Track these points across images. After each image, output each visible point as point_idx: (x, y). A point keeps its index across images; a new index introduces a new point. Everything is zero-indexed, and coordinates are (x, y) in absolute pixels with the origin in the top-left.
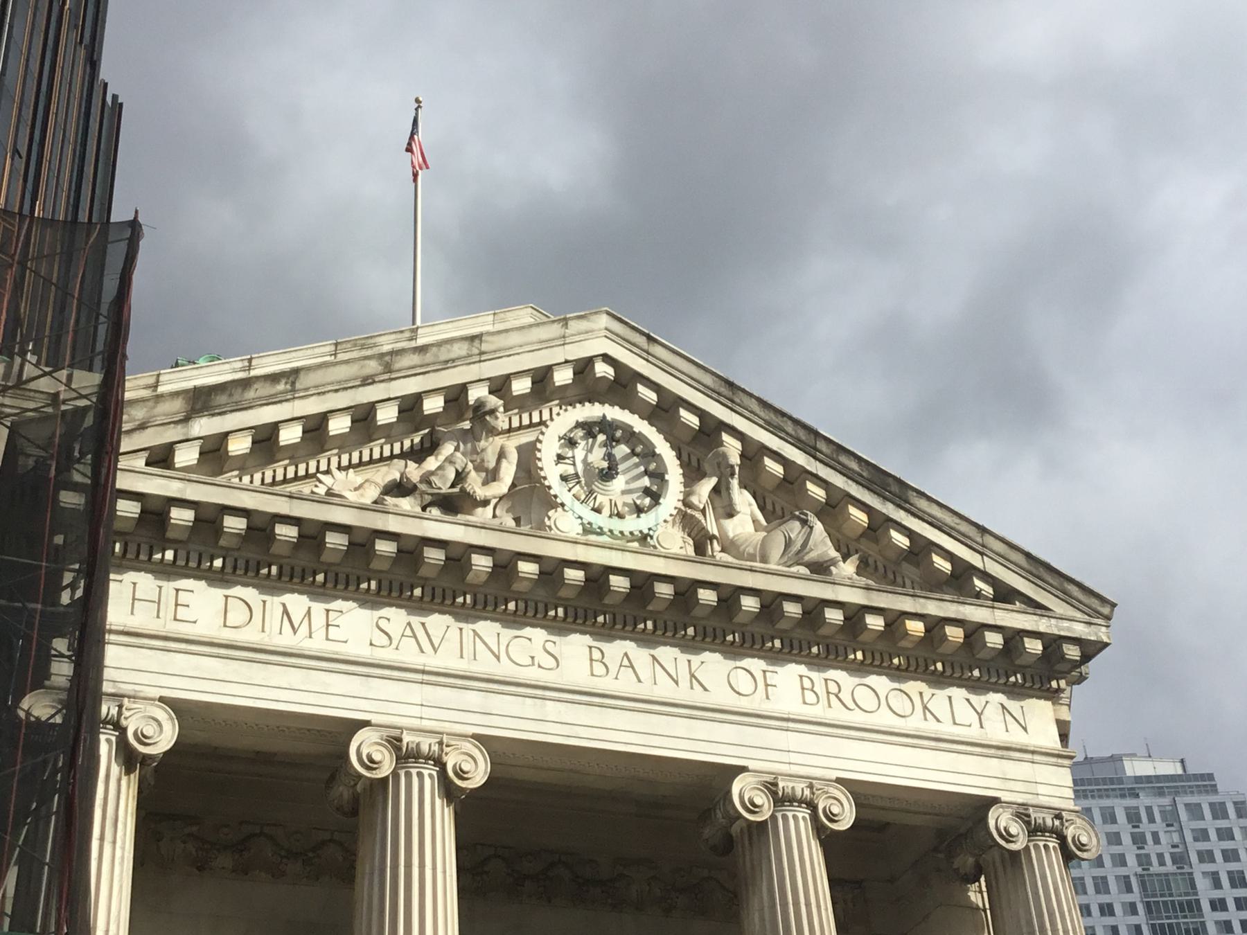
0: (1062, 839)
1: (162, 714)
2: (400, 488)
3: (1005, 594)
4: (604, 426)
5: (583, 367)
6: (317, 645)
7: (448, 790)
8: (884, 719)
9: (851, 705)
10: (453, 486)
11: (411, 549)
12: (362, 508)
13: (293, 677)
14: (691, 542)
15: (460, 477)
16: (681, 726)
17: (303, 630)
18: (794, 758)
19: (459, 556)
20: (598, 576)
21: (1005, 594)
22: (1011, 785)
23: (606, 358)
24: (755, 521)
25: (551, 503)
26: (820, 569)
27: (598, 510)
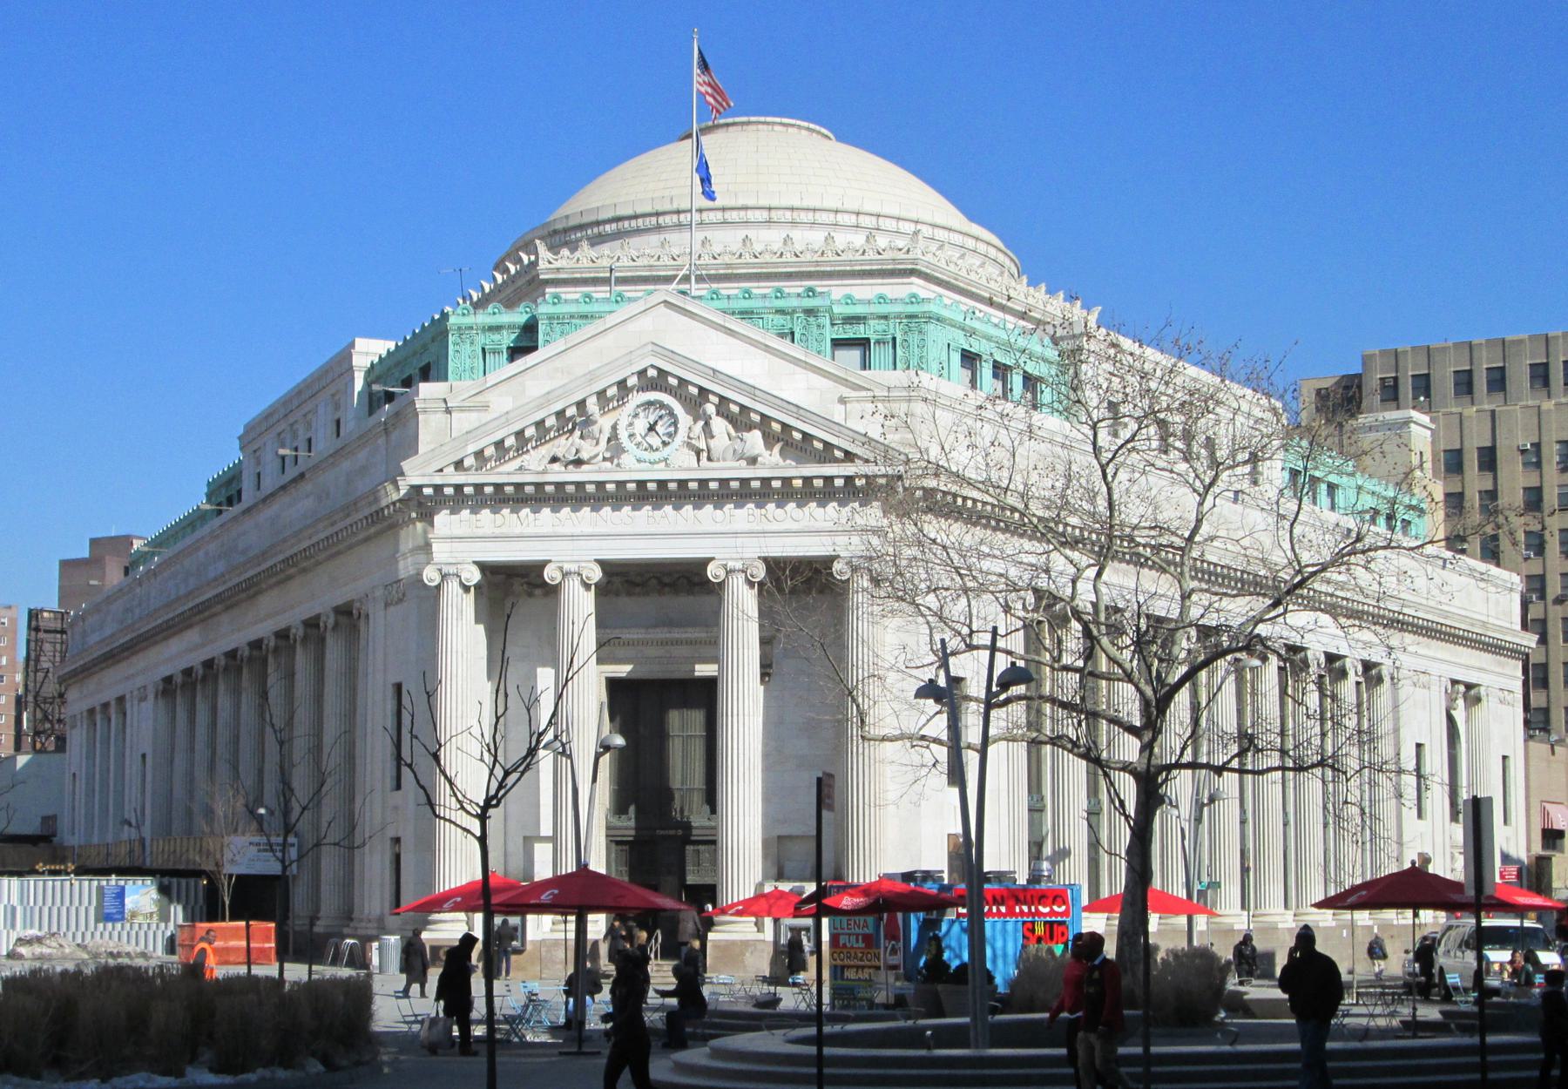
2: (554, 460)
3: (849, 456)
4: (650, 404)
5: (642, 373)
11: (560, 486)
12: (538, 473)
15: (577, 451)
19: (580, 485)
20: (641, 484)
21: (849, 456)
23: (652, 366)
24: (729, 435)
25: (624, 451)
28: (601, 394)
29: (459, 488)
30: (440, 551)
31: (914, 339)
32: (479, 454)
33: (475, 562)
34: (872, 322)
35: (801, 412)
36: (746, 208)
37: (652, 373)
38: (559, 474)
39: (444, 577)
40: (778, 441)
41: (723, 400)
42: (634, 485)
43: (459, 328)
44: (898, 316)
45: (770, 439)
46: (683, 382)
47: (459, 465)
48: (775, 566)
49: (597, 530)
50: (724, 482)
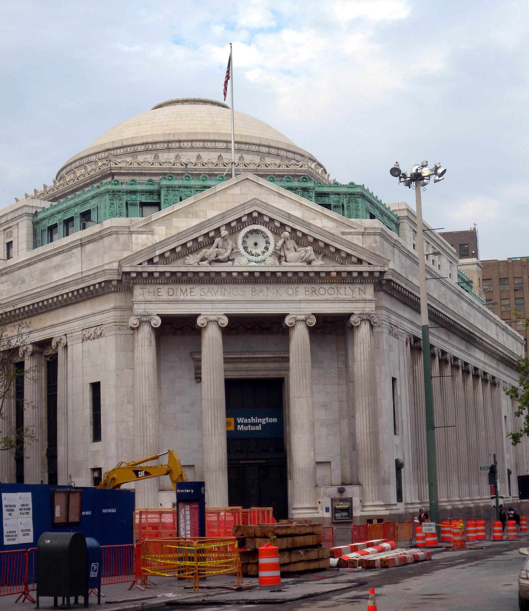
0: (370, 321)
1: (158, 318)
2: (203, 259)
3: (360, 261)
5: (250, 215)
6: (189, 298)
7: (220, 327)
8: (327, 297)
9: (318, 294)
10: (216, 257)
11: (207, 273)
13: (184, 306)
14: (277, 258)
16: (272, 306)
17: (185, 294)
18: (302, 310)
20: (252, 273)
21: (360, 261)
22: (358, 309)
26: (309, 263)
27: (253, 255)
28: (228, 225)
29: (151, 274)
30: (139, 309)
31: (353, 205)
32: (162, 255)
33: (157, 315)
34: (332, 196)
35: (332, 239)
36: (215, 141)
37: (255, 215)
38: (205, 267)
39: (141, 322)
40: (320, 253)
41: (294, 230)
42: (248, 274)
43: (113, 191)
44: (345, 194)
45: (317, 252)
46: (272, 220)
47: (151, 261)
48: (321, 318)
49: (226, 298)
50: (295, 273)
